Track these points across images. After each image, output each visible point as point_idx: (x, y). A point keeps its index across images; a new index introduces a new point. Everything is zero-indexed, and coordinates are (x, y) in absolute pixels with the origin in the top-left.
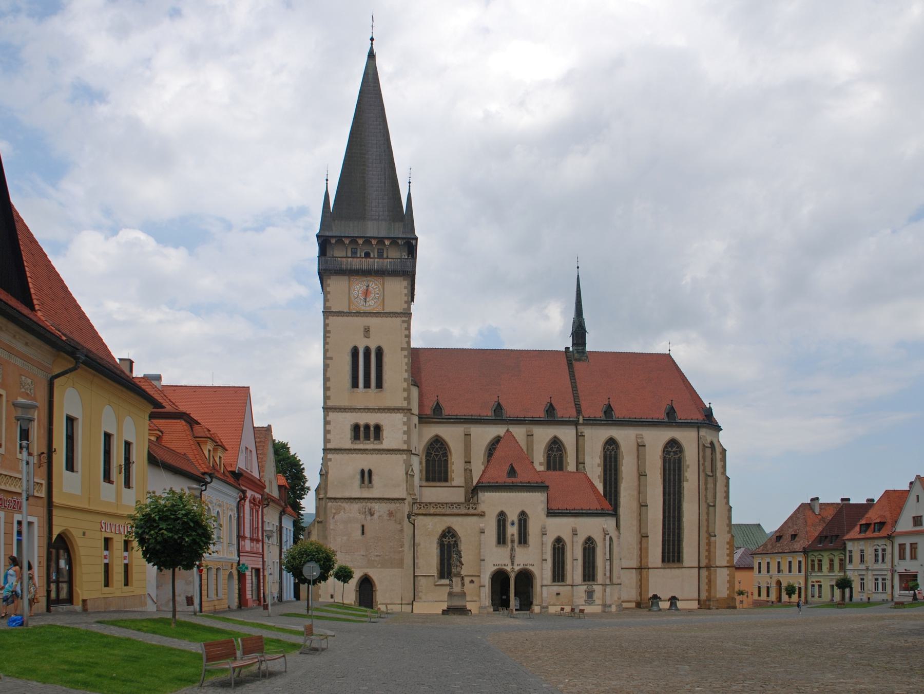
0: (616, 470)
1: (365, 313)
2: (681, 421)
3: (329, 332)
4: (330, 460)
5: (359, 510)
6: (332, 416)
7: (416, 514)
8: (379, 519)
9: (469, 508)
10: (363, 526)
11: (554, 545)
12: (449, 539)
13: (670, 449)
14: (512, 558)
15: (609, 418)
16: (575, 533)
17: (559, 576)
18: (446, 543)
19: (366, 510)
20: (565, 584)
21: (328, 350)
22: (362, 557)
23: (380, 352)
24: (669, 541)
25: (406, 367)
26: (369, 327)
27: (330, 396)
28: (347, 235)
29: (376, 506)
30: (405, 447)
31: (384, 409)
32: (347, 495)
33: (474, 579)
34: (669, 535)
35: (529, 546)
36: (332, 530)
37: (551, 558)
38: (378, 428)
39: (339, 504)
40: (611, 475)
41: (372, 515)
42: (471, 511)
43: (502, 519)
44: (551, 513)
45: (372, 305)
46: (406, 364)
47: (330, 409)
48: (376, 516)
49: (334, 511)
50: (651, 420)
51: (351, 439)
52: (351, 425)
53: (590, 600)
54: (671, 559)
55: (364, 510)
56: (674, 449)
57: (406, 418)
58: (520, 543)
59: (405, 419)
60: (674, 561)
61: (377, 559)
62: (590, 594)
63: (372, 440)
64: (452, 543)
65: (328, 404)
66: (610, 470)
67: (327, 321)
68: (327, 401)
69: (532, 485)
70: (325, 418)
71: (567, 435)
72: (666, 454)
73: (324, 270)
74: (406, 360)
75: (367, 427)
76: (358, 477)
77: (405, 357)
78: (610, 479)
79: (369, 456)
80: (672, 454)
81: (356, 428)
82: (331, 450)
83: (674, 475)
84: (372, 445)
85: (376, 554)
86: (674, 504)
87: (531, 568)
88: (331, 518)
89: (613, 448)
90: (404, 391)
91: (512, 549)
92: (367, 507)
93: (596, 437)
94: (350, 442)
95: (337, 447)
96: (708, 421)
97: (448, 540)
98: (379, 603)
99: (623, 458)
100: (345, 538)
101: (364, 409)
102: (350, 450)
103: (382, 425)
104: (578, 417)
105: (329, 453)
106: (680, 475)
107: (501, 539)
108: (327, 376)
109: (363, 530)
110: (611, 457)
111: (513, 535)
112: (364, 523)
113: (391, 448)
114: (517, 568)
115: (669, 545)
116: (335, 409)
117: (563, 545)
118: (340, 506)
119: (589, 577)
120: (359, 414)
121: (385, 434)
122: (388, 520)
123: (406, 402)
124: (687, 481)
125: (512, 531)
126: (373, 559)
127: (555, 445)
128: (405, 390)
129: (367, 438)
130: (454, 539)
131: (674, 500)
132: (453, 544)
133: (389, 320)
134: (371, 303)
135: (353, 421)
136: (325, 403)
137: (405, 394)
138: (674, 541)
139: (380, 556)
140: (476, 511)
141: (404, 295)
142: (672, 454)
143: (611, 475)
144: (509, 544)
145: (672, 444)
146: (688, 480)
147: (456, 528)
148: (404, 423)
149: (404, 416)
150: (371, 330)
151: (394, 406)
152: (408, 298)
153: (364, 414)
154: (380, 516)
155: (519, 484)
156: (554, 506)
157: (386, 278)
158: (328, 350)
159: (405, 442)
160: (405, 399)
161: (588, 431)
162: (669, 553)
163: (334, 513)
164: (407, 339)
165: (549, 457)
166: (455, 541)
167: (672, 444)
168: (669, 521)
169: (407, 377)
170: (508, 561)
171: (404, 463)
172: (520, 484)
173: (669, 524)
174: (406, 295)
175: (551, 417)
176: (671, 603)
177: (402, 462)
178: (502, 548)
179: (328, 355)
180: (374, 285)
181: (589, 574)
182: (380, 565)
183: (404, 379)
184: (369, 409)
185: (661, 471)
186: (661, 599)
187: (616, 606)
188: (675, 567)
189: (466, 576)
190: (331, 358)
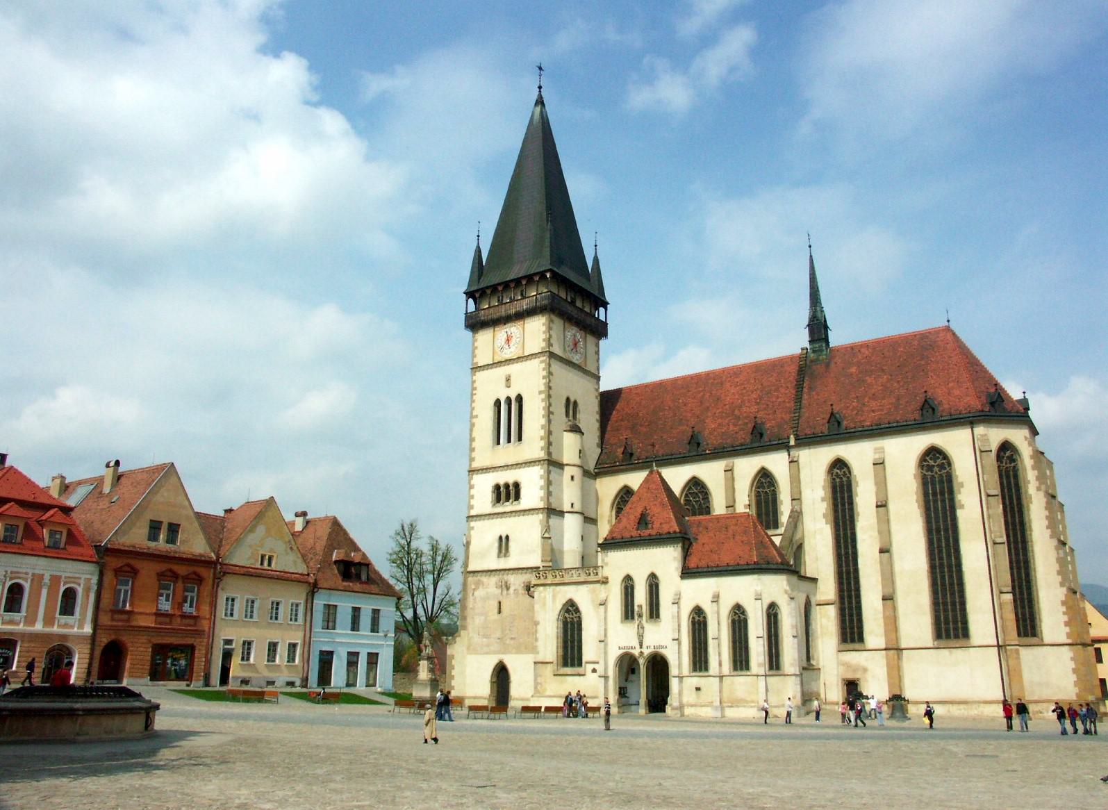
0: (851, 503)
1: (506, 361)
2: (943, 419)
4: (473, 528)
5: (496, 584)
6: (477, 479)
7: (535, 585)
8: (514, 593)
10: (500, 603)
11: (693, 618)
12: (573, 614)
13: (932, 463)
15: (837, 431)
16: (716, 599)
17: (701, 663)
18: (569, 620)
20: (706, 674)
22: (498, 641)
23: (520, 399)
24: (945, 604)
25: (543, 412)
26: (510, 377)
30: (541, 505)
31: (522, 464)
32: (486, 567)
33: (596, 666)
34: (944, 596)
36: (471, 608)
38: (517, 485)
39: (479, 577)
40: (843, 510)
41: (508, 589)
42: (592, 578)
44: (688, 572)
46: (544, 408)
47: (473, 471)
48: (511, 590)
49: (473, 587)
50: (905, 423)
51: (492, 502)
54: (952, 634)
56: (939, 462)
57: (543, 470)
58: (651, 616)
59: (542, 472)
60: (956, 637)
61: (512, 642)
63: (511, 501)
64: (575, 620)
66: (843, 505)
67: (474, 378)
71: (776, 462)
72: (927, 472)
74: (543, 404)
75: (507, 486)
76: (496, 545)
78: (844, 516)
79: (508, 519)
80: (936, 469)
82: (472, 516)
83: (943, 501)
85: (513, 636)
86: (948, 545)
87: (663, 651)
88: (471, 595)
89: (844, 472)
90: (541, 439)
91: (640, 627)
92: (503, 583)
93: (816, 460)
94: (491, 505)
95: (480, 513)
96: (1019, 415)
97: (571, 616)
98: (513, 698)
99: (857, 486)
100: (483, 618)
101: (503, 466)
104: (788, 438)
105: (472, 521)
106: (952, 500)
107: (629, 612)
109: (500, 608)
110: (842, 486)
111: (640, 606)
112: (501, 599)
113: (527, 508)
114: (647, 652)
115: (945, 610)
116: (478, 470)
117: (705, 618)
118: (479, 580)
119: (741, 662)
123: (543, 452)
124: (962, 507)
127: (764, 480)
129: (508, 499)
131: (947, 540)
133: (528, 362)
134: (513, 349)
135: (493, 483)
136: (470, 465)
137: (542, 443)
138: (954, 604)
142: (936, 469)
143: (843, 510)
144: (636, 617)
145: (934, 455)
146: (963, 505)
147: (578, 600)
148: (541, 477)
149: (541, 469)
150: (512, 378)
156: (693, 562)
158: (474, 408)
159: (542, 499)
161: (805, 455)
162: (947, 623)
164: (545, 381)
165: (758, 495)
166: (580, 618)
167: (934, 455)
168: (942, 572)
169: (543, 423)
170: (635, 643)
173: (943, 577)
174: (544, 332)
175: (759, 441)
176: (893, 706)
180: (514, 329)
181: (741, 660)
184: (507, 466)
185: (918, 497)
188: (957, 646)
189: (587, 663)
190: (477, 416)
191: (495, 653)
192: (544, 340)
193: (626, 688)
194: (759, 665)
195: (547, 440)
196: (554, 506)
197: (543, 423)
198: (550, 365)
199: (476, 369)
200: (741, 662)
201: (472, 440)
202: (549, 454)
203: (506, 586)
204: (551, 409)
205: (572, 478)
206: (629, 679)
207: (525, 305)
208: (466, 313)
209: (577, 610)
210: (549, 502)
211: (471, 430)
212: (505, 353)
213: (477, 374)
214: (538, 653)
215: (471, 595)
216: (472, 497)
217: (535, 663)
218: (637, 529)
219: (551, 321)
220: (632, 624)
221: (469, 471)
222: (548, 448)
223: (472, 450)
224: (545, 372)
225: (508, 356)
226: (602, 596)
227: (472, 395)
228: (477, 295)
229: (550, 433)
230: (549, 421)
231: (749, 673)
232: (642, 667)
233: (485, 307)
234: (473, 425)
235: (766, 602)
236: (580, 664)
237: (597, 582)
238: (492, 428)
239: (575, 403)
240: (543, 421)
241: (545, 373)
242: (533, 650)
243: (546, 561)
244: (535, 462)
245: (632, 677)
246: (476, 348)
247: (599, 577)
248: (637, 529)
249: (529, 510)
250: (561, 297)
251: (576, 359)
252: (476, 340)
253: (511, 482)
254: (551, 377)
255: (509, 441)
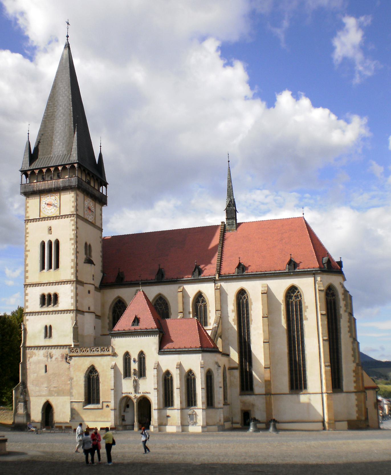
1: (48, 217)
3: (28, 233)
4: (28, 320)
5: (44, 354)
6: (29, 290)
9: (104, 350)
10: (46, 366)
11: (165, 377)
14: (136, 388)
19: (48, 354)
21: (27, 245)
22: (46, 388)
23: (57, 242)
25: (72, 252)
26: (50, 227)
27: (28, 277)
28: (37, 167)
29: (54, 351)
30: (72, 308)
32: (37, 344)
33: (108, 404)
35: (146, 379)
37: (163, 387)
38: (56, 296)
41: (51, 357)
42: (106, 353)
43: (127, 357)
45: (51, 211)
46: (73, 249)
48: (54, 358)
51: (40, 305)
52: (40, 295)
53: (192, 421)
55: (47, 354)
57: (72, 287)
59: (72, 288)
61: (55, 389)
62: (193, 416)
63: (52, 304)
65: (27, 282)
67: (27, 226)
68: (27, 280)
69: (148, 330)
70: (25, 292)
73: (24, 192)
74: (73, 247)
75: (49, 295)
76: (43, 331)
81: (43, 297)
82: (27, 313)
84: (52, 308)
85: (55, 386)
87: (148, 396)
91: (135, 381)
94: (39, 306)
95: (32, 311)
100: (36, 375)
102: (39, 313)
103: (58, 294)
107: (127, 374)
108: (27, 263)
112: (47, 364)
113: (63, 309)
114: (138, 395)
117: (171, 377)
118: (33, 352)
120: (45, 287)
121: (60, 299)
122: (61, 361)
123: (73, 276)
125: (134, 366)
126: (52, 389)
130: (97, 374)
132: (97, 378)
133: (63, 220)
135: (41, 293)
139: (56, 387)
140: (109, 352)
141: (72, 202)
148: (72, 291)
151: (65, 280)
152: (74, 204)
153: (48, 287)
154: (56, 358)
155: (139, 331)
157: (61, 192)
158: (27, 245)
159: (72, 304)
160: (72, 274)
163: (30, 357)
164: (74, 232)
166: (98, 376)
169: (73, 258)
170: (132, 390)
171: (71, 319)
172: (140, 331)
177: (70, 319)
178: (128, 380)
179: (28, 249)
182: (56, 395)
183: (72, 259)
184: (50, 283)
186: (260, 421)
187: (218, 427)
189: (103, 402)
190: (29, 251)
191: (44, 396)
192: (73, 207)
193: (124, 416)
194: (203, 403)
195: (75, 269)
196: (79, 308)
197: (73, 258)
198: (77, 223)
199: (28, 221)
200: (192, 402)
201: (26, 265)
202: (77, 277)
203: (50, 356)
204: (78, 250)
205: (89, 292)
206: (126, 411)
207: (60, 182)
208: (21, 184)
209: (96, 371)
210: (77, 307)
211: (25, 259)
212: (48, 213)
213: (29, 223)
214: (73, 396)
215: (27, 361)
216: (27, 301)
217: (71, 402)
218: (133, 325)
219: (77, 195)
220: (130, 380)
221: (25, 285)
222: (76, 274)
223: (26, 271)
224: (74, 226)
225: (50, 215)
226: (113, 363)
227: (26, 237)
228: (29, 173)
229: (77, 264)
230: (77, 257)
231: (196, 408)
232: (135, 404)
233: (34, 182)
234: (26, 256)
235: (207, 368)
236: (98, 402)
237: (109, 355)
238: (40, 259)
239: (90, 246)
240: (73, 257)
241: (74, 227)
242: (71, 394)
243: (76, 342)
244: (68, 282)
245: (128, 410)
246: (28, 207)
247: (110, 352)
248: (133, 325)
249: (64, 311)
250: (83, 180)
251: (90, 218)
252: (28, 202)
253: (52, 293)
254: (77, 230)
255: (50, 267)
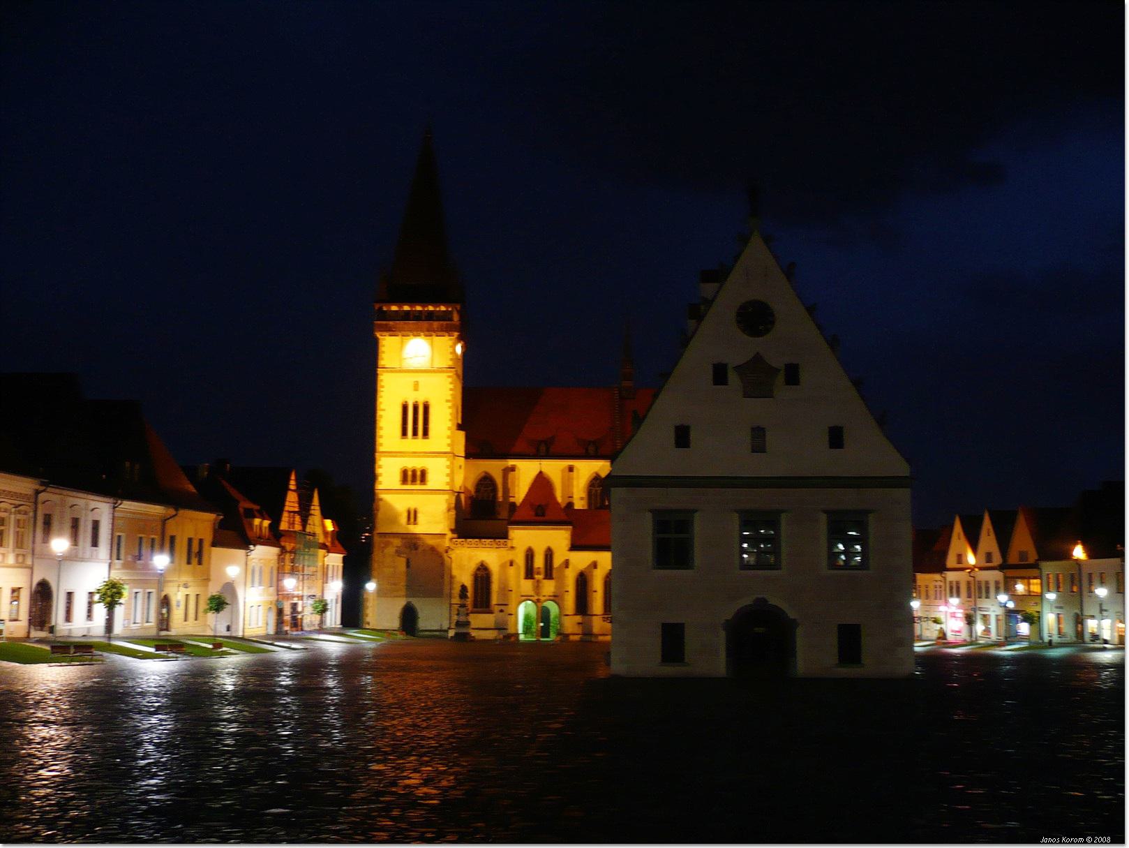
25: (449, 417)
38: (423, 473)
41: (416, 549)
44: (574, 547)
46: (451, 414)
59: (448, 463)
75: (414, 472)
77: (450, 407)
100: (392, 570)
107: (530, 573)
121: (430, 477)
128: (448, 437)
129: (414, 481)
137: (449, 441)
159: (448, 484)
163: (383, 547)
164: (451, 392)
169: (450, 425)
190: (383, 410)
197: (450, 425)
202: (452, 449)
